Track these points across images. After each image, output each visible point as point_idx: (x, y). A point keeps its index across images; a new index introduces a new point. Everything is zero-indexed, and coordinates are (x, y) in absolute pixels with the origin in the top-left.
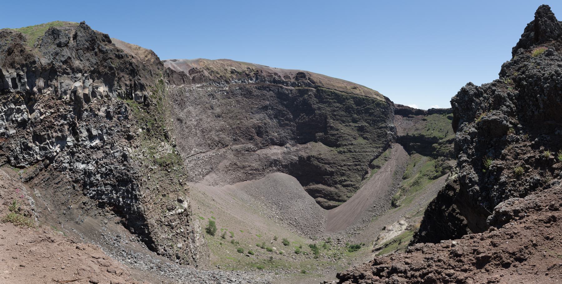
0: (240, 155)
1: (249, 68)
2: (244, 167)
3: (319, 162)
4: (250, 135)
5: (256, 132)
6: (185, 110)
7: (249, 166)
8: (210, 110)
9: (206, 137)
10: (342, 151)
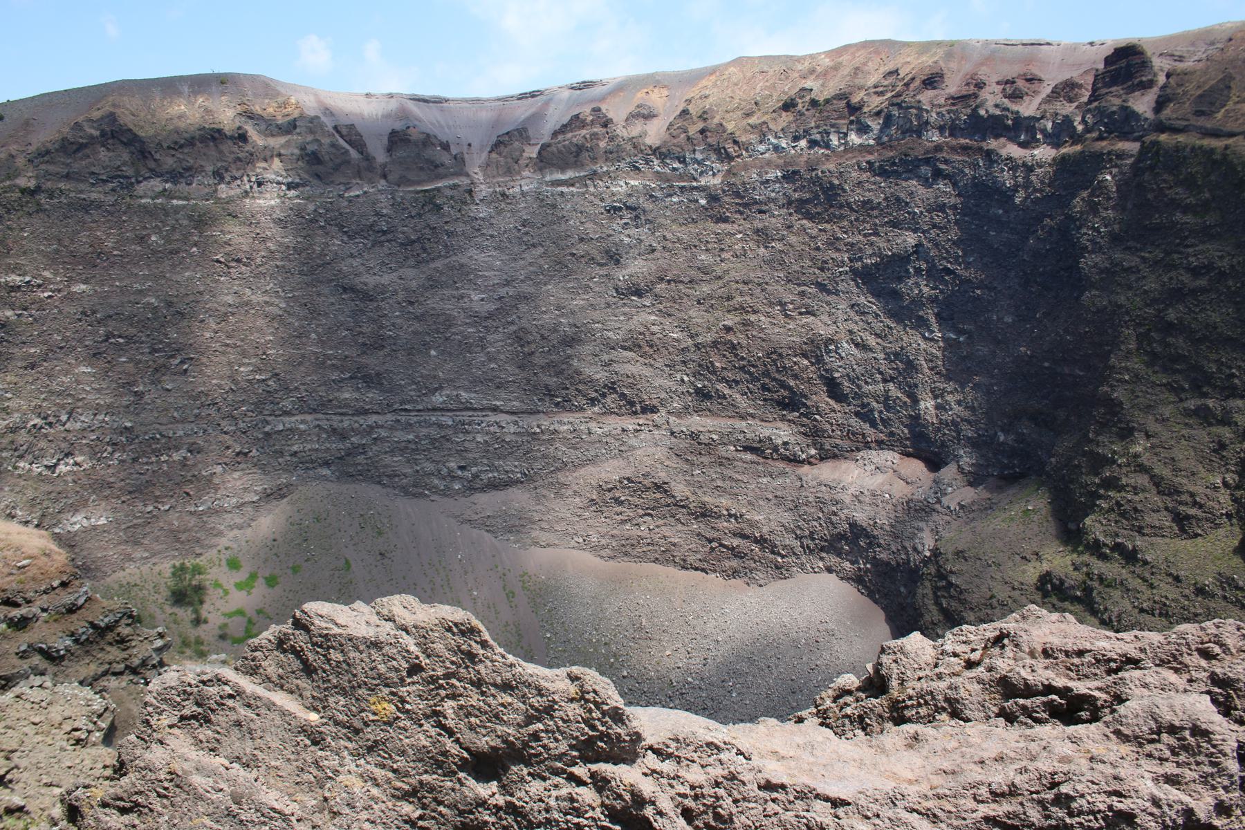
0: (704, 459)
1: (897, 71)
2: (704, 514)
3: (936, 589)
4: (783, 385)
5: (821, 377)
6: (438, 264)
7: (736, 519)
8: (601, 265)
9: (538, 360)
10: (1051, 581)
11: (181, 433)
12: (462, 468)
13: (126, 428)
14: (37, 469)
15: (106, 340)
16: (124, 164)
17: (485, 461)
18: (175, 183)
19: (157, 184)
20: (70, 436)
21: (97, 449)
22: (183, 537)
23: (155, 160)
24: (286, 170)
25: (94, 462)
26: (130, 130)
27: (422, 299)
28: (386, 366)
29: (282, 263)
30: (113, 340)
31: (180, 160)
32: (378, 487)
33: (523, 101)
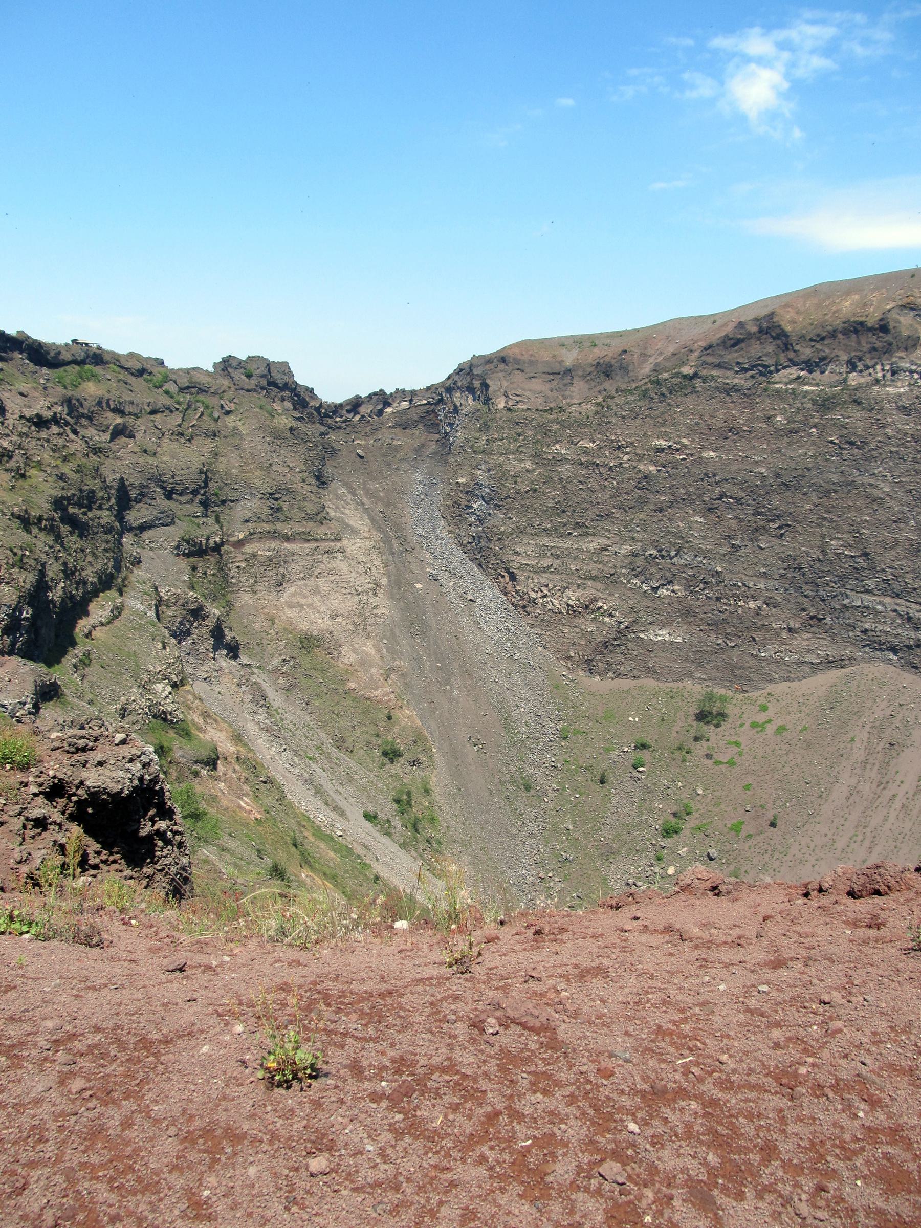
11: (762, 586)
13: (717, 572)
14: (645, 587)
15: (720, 499)
16: (767, 355)
18: (810, 372)
19: (793, 372)
20: (674, 569)
21: (691, 583)
22: (738, 672)
23: (795, 351)
25: (687, 593)
26: (779, 326)
29: (897, 449)
30: (725, 500)
31: (818, 351)
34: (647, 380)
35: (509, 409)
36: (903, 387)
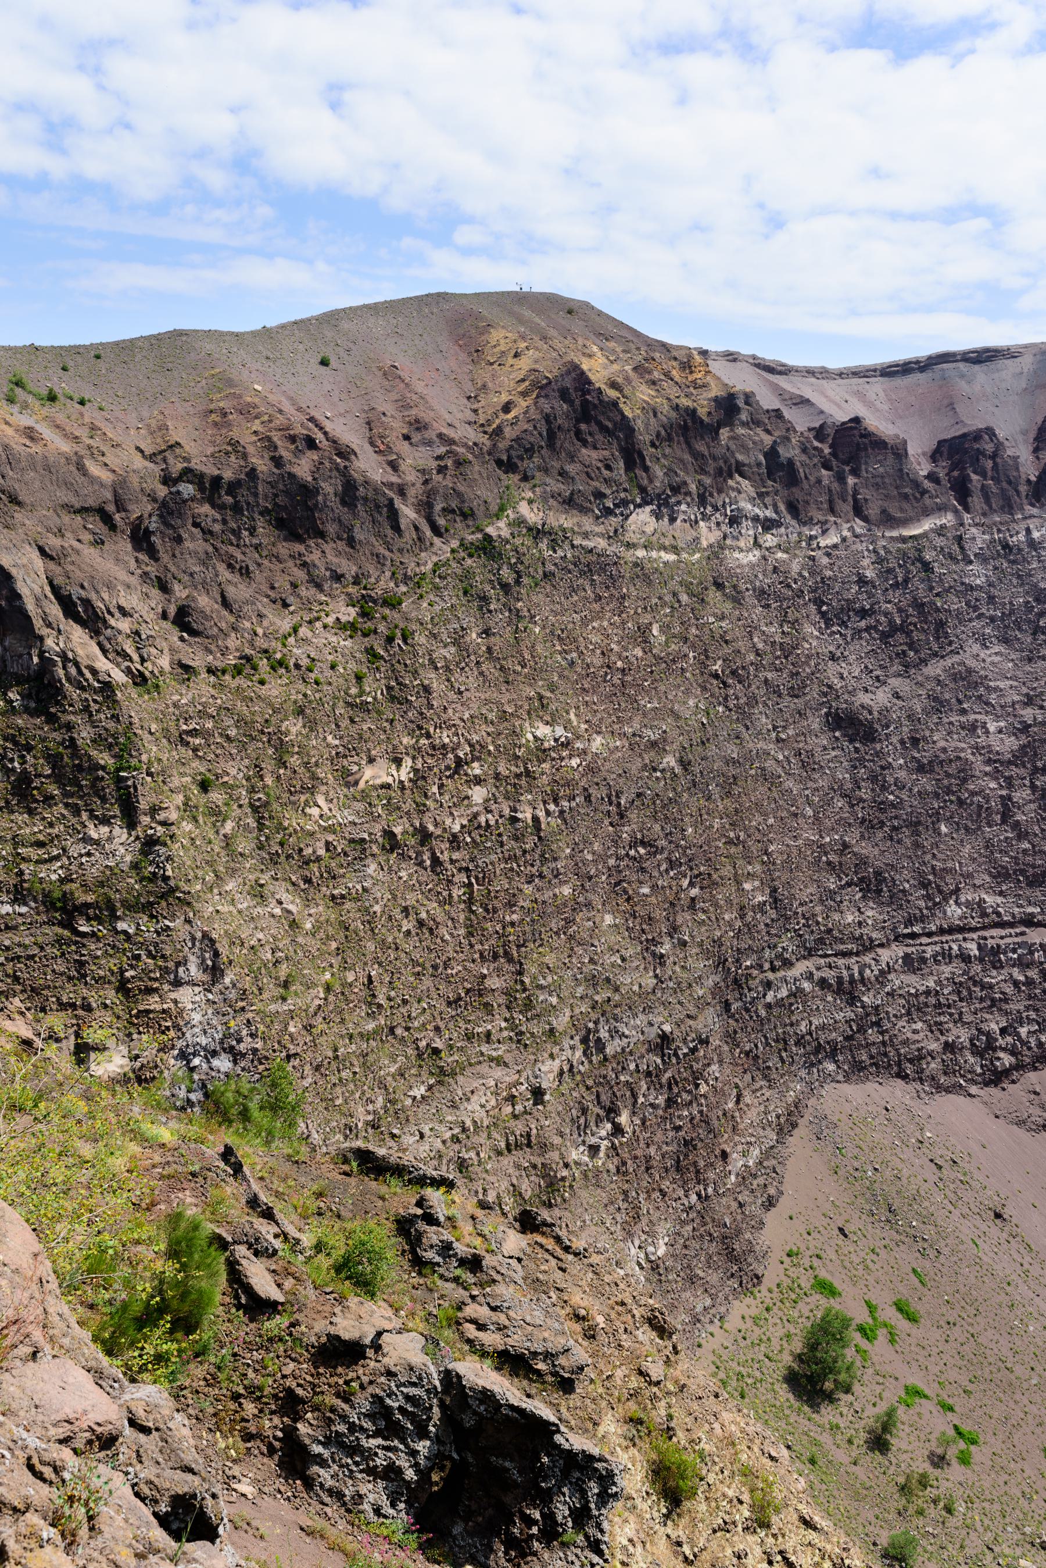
6: (935, 669)
12: (1003, 1031)
17: (1033, 1015)
18: (657, 519)
23: (646, 469)
24: (761, 495)
27: (927, 733)
28: (889, 858)
32: (899, 1081)
33: (900, 382)
34: (455, 544)
35: (140, 680)
36: (749, 550)
